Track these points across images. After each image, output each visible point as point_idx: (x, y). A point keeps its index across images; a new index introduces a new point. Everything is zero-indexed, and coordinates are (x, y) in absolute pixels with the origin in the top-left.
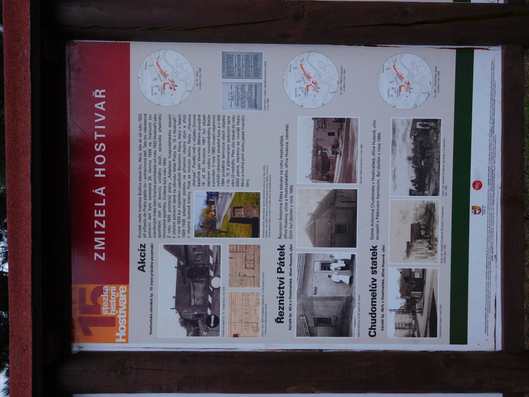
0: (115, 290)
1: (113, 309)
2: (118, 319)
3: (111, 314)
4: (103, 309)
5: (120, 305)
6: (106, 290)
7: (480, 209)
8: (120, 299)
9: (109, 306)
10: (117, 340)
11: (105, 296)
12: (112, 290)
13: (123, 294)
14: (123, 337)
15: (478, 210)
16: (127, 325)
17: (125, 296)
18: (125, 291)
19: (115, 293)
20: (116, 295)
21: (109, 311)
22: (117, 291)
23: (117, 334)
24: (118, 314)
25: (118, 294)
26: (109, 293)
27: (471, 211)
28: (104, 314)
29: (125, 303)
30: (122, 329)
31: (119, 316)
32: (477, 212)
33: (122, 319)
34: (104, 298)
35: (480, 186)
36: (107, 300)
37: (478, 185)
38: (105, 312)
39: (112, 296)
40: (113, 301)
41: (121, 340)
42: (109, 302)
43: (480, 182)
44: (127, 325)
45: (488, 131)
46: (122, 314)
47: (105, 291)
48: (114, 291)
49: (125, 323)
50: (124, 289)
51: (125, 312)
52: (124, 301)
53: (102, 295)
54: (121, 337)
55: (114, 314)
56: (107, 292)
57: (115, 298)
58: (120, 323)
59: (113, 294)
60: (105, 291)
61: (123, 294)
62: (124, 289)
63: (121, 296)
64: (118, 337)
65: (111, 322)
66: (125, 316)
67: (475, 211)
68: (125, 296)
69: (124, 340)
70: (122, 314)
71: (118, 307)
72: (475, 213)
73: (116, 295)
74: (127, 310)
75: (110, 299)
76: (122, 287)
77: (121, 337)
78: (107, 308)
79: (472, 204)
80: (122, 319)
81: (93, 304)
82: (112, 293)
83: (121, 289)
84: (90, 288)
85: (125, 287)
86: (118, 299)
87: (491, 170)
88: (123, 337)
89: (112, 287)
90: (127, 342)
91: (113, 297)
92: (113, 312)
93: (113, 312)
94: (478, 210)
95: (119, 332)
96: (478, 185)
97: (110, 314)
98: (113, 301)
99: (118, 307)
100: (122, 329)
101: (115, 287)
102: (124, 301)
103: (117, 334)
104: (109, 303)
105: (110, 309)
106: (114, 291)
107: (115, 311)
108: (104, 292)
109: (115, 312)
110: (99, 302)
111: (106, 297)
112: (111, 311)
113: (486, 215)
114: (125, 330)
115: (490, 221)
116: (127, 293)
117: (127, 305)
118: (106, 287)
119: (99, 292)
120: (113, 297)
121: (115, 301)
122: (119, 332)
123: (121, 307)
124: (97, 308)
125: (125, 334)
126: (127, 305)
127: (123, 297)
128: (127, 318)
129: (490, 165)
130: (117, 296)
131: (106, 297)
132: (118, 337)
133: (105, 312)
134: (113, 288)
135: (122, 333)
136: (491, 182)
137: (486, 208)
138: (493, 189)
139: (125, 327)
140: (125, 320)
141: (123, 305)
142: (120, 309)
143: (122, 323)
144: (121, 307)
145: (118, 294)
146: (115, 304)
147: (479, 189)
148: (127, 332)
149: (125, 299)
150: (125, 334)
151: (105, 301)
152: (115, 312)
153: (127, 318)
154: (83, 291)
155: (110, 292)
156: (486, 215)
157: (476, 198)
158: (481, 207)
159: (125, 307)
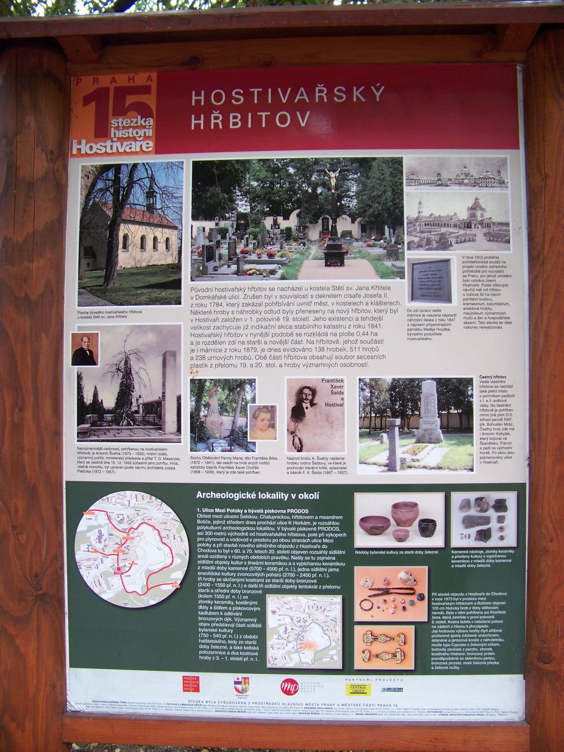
0: (147, 135)
2: (105, 142)
3: (113, 131)
4: (120, 120)
5: (125, 143)
6: (147, 123)
8: (133, 143)
9: (124, 128)
12: (147, 131)
13: (141, 146)
17: (138, 149)
18: (145, 149)
19: (143, 135)
20: (140, 137)
21: (117, 128)
22: (146, 138)
24: (112, 141)
28: (112, 122)
29: (128, 150)
33: (105, 147)
34: (135, 120)
36: (132, 125)
39: (139, 131)
42: (130, 127)
43: (295, 692)
46: (112, 146)
47: (145, 121)
48: (145, 133)
50: (147, 148)
51: (115, 150)
52: (130, 148)
53: (139, 117)
55: (112, 136)
56: (143, 124)
57: (135, 135)
58: (99, 144)
59: (141, 132)
60: (145, 121)
61: (141, 146)
62: (147, 148)
63: (138, 144)
66: (109, 151)
70: (112, 146)
73: (140, 137)
75: (134, 128)
76: (151, 144)
78: (120, 125)
80: (105, 147)
82: (143, 131)
83: (148, 144)
84: (151, 100)
86: (134, 139)
89: (151, 130)
91: (137, 133)
92: (115, 133)
93: (115, 133)
97: (113, 129)
100: (91, 148)
101: (151, 135)
102: (130, 148)
103: (84, 142)
104: (128, 128)
106: (145, 133)
107: (117, 136)
108: (144, 119)
109: (115, 137)
111: (137, 123)
112: (117, 132)
114: (89, 152)
118: (151, 121)
119: (145, 112)
120: (137, 133)
121: (131, 136)
124: (121, 112)
130: (138, 139)
133: (114, 122)
141: (125, 147)
142: (119, 144)
145: (141, 138)
146: (127, 135)
147: (282, 689)
149: (133, 150)
151: (132, 122)
152: (115, 137)
153: (106, 154)
154: (146, 90)
155: (144, 127)
159: (121, 150)
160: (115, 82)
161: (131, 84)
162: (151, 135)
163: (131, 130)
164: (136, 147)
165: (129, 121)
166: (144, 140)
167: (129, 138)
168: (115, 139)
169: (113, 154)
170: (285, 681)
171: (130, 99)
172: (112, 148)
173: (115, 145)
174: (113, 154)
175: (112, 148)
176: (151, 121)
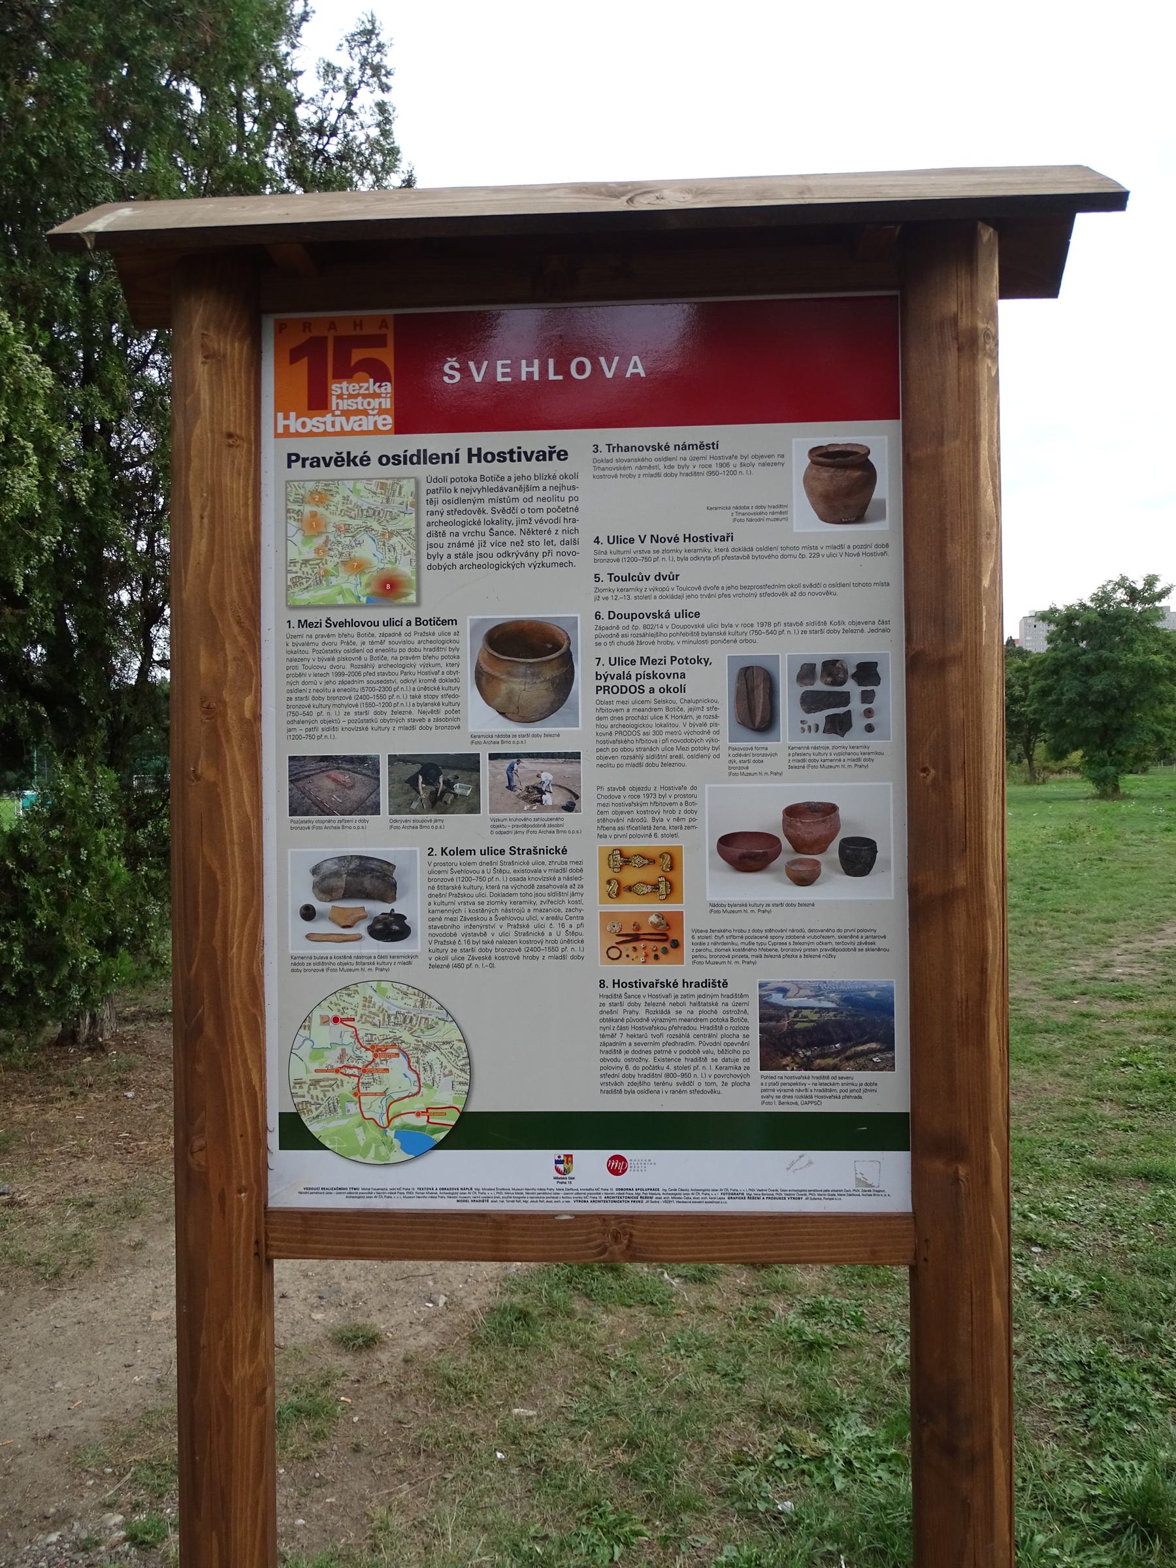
1: (344, 405)
3: (334, 400)
4: (345, 384)
5: (353, 419)
7: (566, 1172)
8: (363, 417)
9: (350, 396)
10: (280, 415)
11: (371, 385)
13: (375, 423)
14: (286, 427)
15: (563, 1168)
16: (311, 434)
17: (371, 428)
20: (373, 409)
21: (340, 397)
22: (381, 411)
23: (293, 415)
24: (334, 415)
25: (375, 412)
26: (375, 395)
27: (562, 1153)
28: (333, 387)
29: (357, 429)
30: (304, 425)
31: (329, 418)
32: (561, 1167)
33: (324, 423)
34: (366, 385)
35: (615, 1172)
36: (362, 391)
37: (617, 1168)
38: (336, 388)
40: (360, 404)
41: (281, 422)
43: (624, 1171)
44: (311, 434)
45: (731, 1186)
46: (333, 423)
47: (380, 386)
49: (315, 430)
50: (384, 425)
51: (338, 429)
52: (360, 426)
53: (371, 381)
54: (286, 422)
55: (334, 408)
56: (378, 391)
58: (316, 419)
59: (375, 403)
60: (380, 386)
61: (375, 423)
62: (384, 425)
64: (286, 418)
65: (318, 402)
66: (330, 429)
67: (561, 1162)
68: (371, 428)
69: (280, 430)
70: (333, 423)
71: (347, 414)
72: (557, 1162)
73: (373, 409)
74: (342, 433)
75: (365, 396)
76: (390, 420)
77: (286, 422)
78: (345, 392)
79: (575, 1153)
80: (324, 423)
81: (353, 361)
84: (386, 356)
85: (389, 427)
86: (365, 413)
87: (649, 1194)
88: (286, 427)
90: (277, 435)
91: (369, 404)
94: (563, 1168)
95: (297, 418)
96: (617, 1168)
97: (334, 398)
98: (360, 404)
99: (347, 414)
100: (304, 425)
101: (388, 406)
102: (360, 426)
103: (293, 415)
104: (356, 396)
105: (342, 399)
110: (357, 375)
111: (367, 389)
112: (340, 401)
113: (554, 1185)
114: (301, 430)
115: (542, 1194)
116: (376, 431)
117: (352, 433)
118: (388, 387)
119: (380, 375)
120: (369, 404)
121: (360, 407)
122: (297, 418)
123: (348, 421)
124: (345, 372)
125: (292, 430)
126: (352, 433)
127: (367, 423)
128: (325, 433)
129: (661, 1192)
131: (367, 389)
132: (286, 418)
133: (336, 388)
134: (387, 403)
135: (295, 424)
136: (623, 1194)
137: (568, 1186)
138: (609, 1199)
139: (306, 430)
140: (321, 430)
141: (353, 424)
142: (343, 419)
143: (314, 423)
144: (348, 421)
148: (298, 434)
149: (364, 428)
150: (292, 430)
153: (325, 433)
155: (378, 396)
156: (554, 1185)
157: (590, 1163)
158: (570, 1175)
159: (347, 428)
160: (335, 329)
161: (358, 332)
162: (388, 406)
163: (360, 399)
164: (367, 423)
165: (357, 387)
166: (379, 414)
167: (357, 412)
168: (338, 413)
169: (335, 434)
170: (612, 1158)
171: (358, 355)
172: (333, 426)
173: (338, 420)
174: (335, 434)
175: (333, 426)
176: (388, 387)
